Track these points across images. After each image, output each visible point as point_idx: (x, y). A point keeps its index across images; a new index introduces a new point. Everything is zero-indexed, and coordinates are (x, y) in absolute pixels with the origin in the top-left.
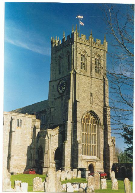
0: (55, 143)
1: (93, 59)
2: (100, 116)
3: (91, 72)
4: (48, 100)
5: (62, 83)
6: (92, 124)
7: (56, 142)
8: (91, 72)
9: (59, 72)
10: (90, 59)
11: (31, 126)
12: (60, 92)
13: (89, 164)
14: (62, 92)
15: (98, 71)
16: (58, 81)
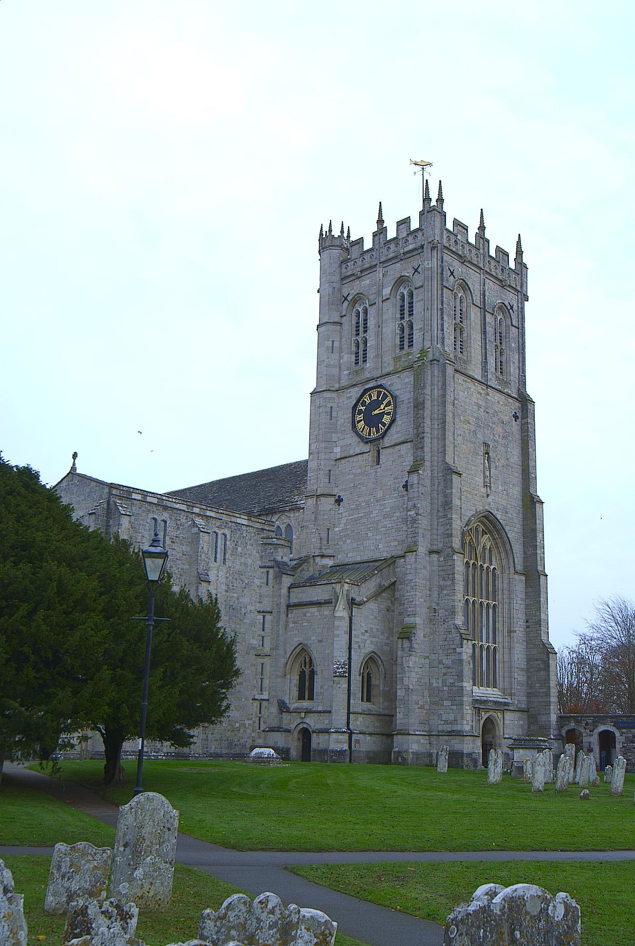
0: (363, 634)
1: (489, 318)
2: (514, 532)
3: (485, 362)
4: (306, 462)
5: (374, 398)
6: (485, 566)
7: (366, 631)
8: (485, 362)
9: (353, 357)
10: (479, 314)
11: (260, 563)
12: (365, 433)
13: (485, 716)
14: (372, 436)
15: (501, 367)
16: (355, 393)
